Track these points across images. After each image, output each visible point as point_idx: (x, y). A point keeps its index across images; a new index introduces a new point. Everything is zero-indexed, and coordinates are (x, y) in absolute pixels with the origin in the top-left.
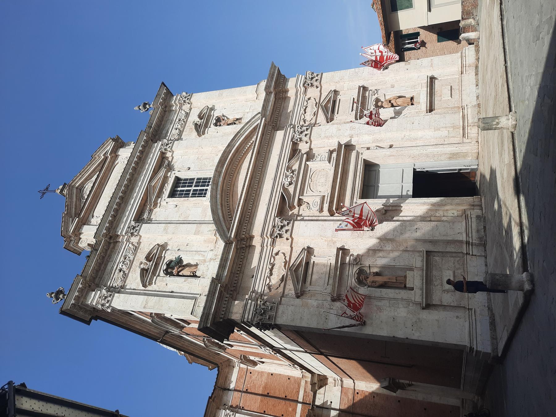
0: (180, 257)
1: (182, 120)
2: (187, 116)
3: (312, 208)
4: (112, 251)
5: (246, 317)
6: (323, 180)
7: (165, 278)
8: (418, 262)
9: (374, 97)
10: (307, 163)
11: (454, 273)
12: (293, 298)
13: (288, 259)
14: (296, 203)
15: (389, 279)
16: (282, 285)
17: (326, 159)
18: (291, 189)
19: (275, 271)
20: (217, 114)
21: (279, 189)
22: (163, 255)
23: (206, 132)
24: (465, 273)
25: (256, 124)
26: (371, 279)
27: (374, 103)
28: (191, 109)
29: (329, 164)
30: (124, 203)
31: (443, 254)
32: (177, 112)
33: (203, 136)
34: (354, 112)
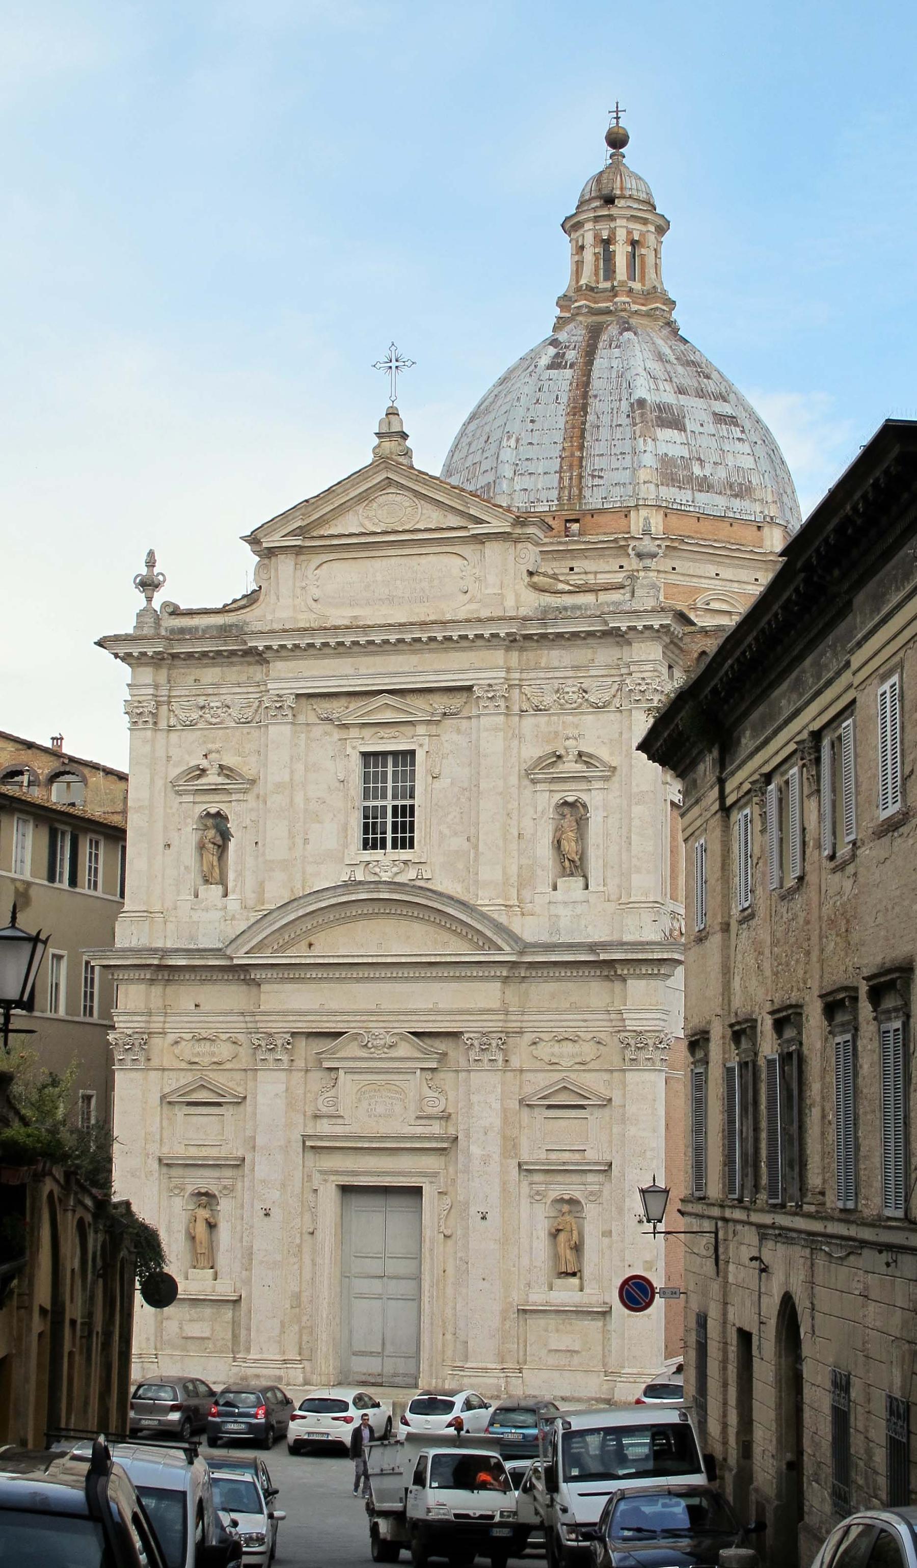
0: (232, 839)
1: (586, 696)
2: (599, 708)
3: (323, 1097)
4: (241, 664)
5: (121, 1018)
6: (380, 1109)
7: (189, 820)
8: (224, 1288)
9: (577, 1195)
10: (418, 1071)
11: (208, 1338)
12: (162, 1089)
13: (228, 1066)
14: (327, 1065)
15: (201, 1243)
16: (184, 1065)
17: (430, 1111)
18: (353, 1050)
19: (205, 1047)
20: (594, 799)
21: (353, 1025)
22: (234, 797)
23: (539, 787)
24: (209, 1353)
25: (500, 942)
26: (203, 1213)
27: (566, 1197)
28: (619, 710)
29: (414, 1117)
30: (336, 651)
31: (235, 1323)
32: (613, 672)
33: (526, 782)
34: (543, 1156)
